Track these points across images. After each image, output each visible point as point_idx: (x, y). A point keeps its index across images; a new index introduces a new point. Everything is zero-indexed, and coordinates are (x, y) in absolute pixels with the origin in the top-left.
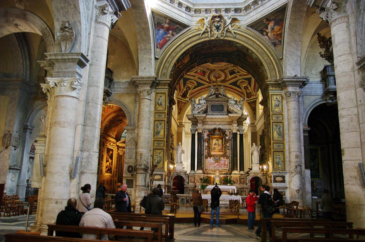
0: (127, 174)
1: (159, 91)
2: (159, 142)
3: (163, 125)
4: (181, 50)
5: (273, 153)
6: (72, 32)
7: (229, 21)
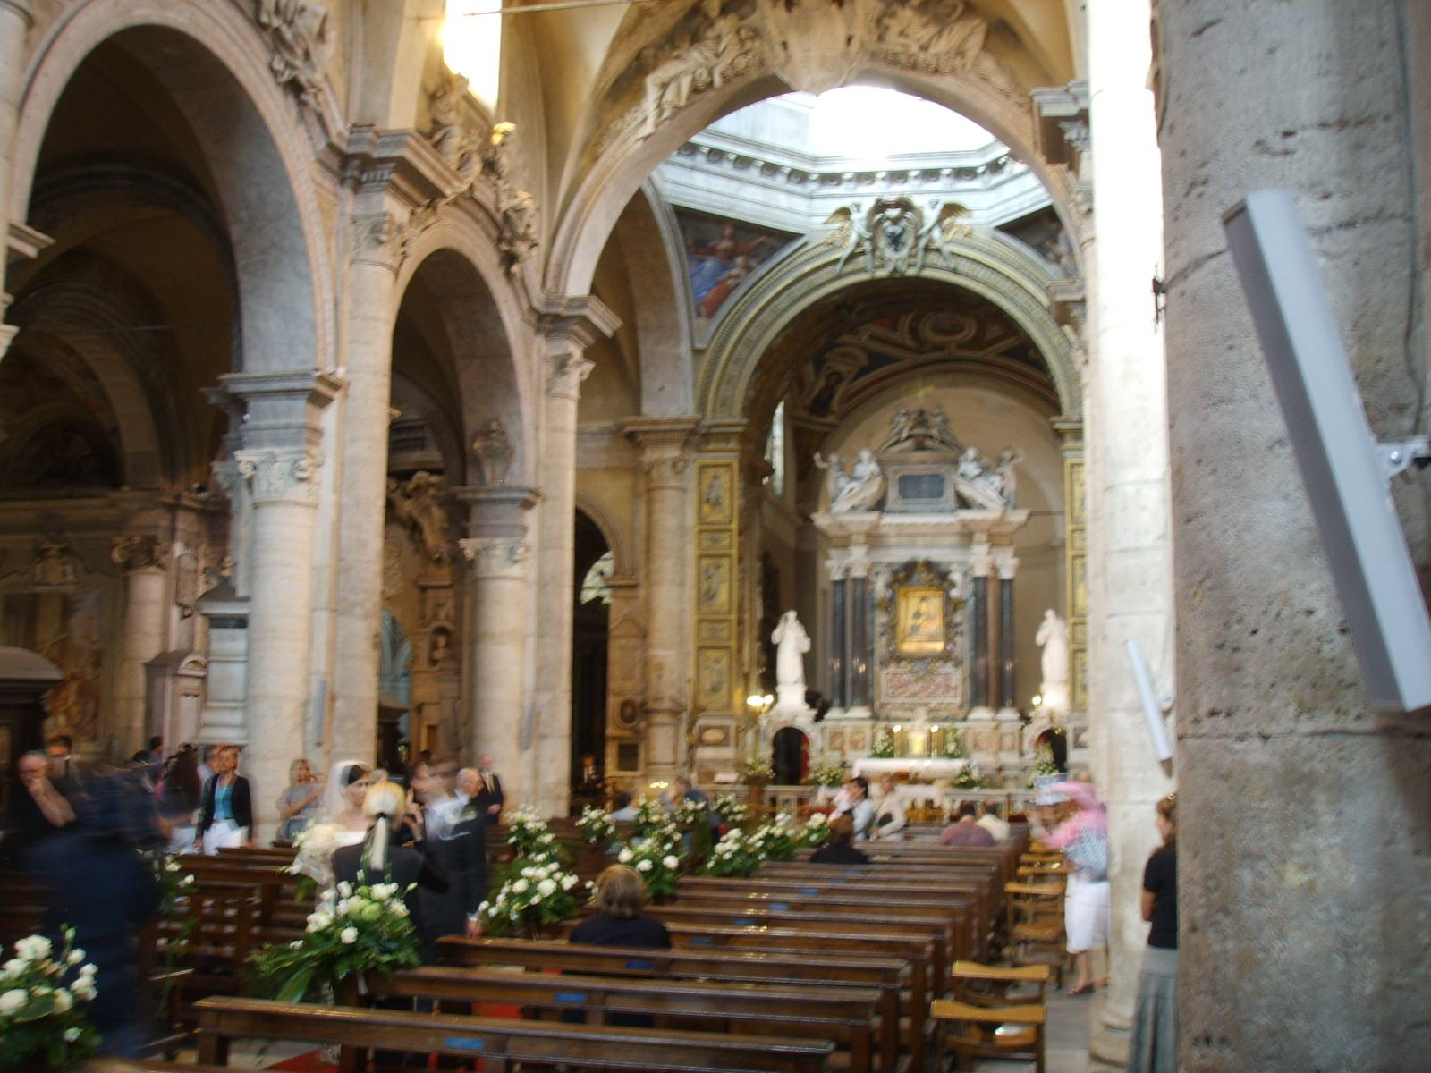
3: (724, 571)
4: (778, 317)
6: (505, 441)
7: (931, 215)
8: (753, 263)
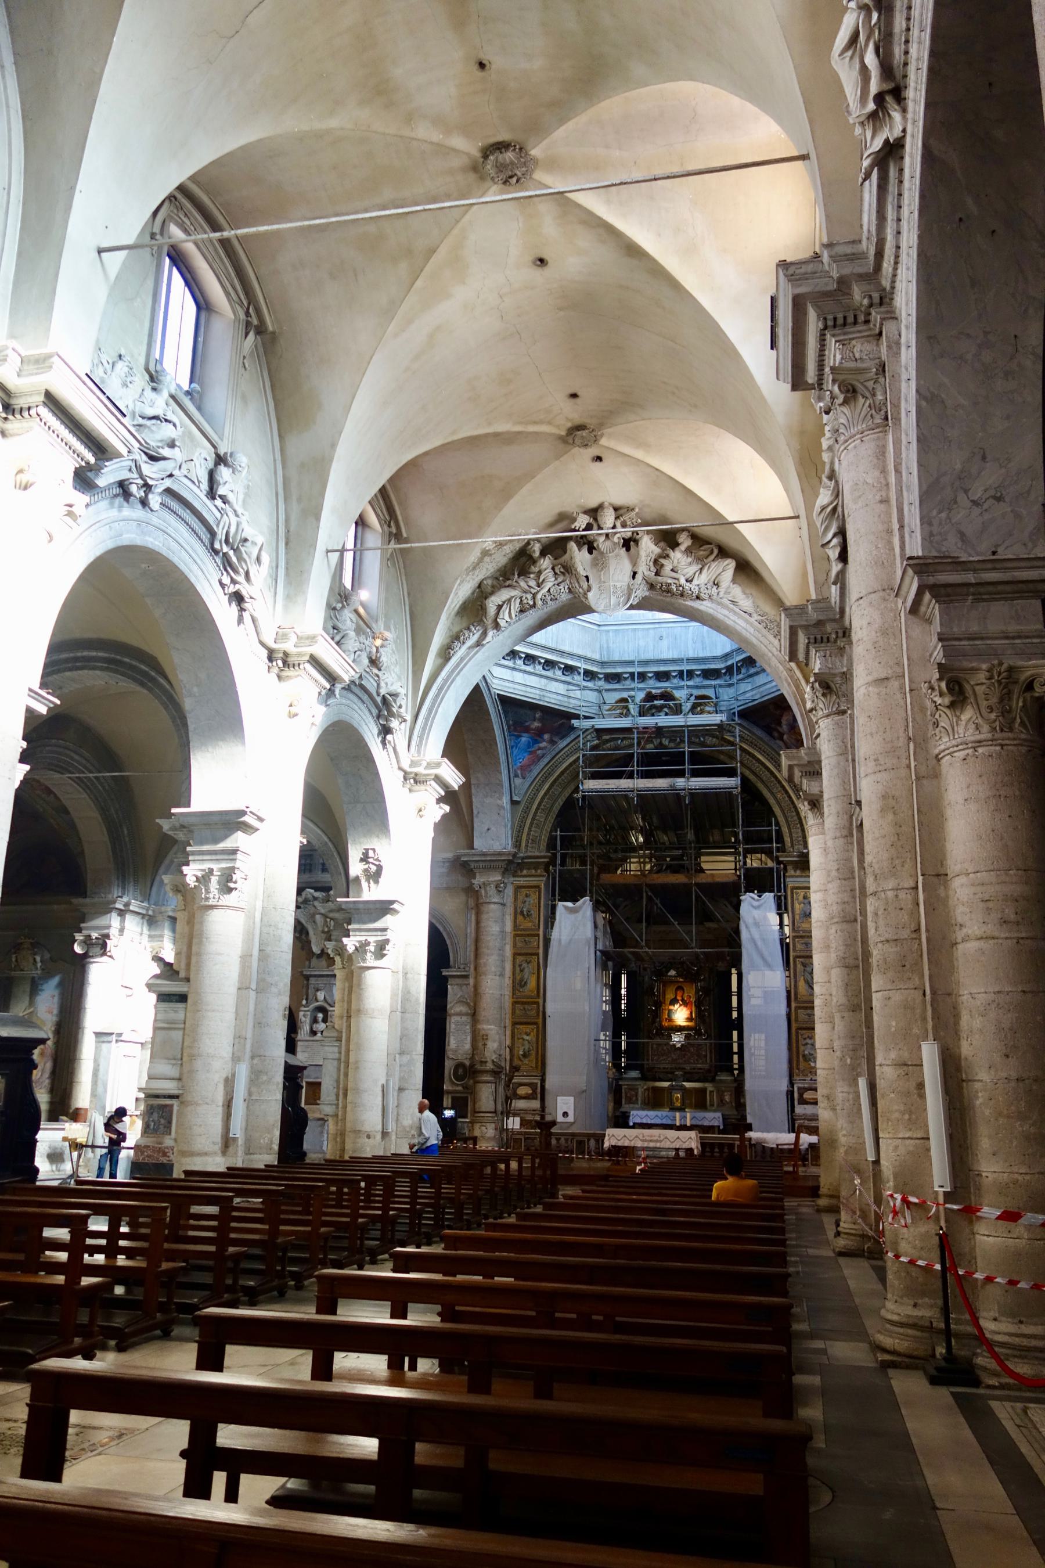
0: (453, 1083)
1: (521, 881)
2: (526, 1007)
5: (797, 1033)
8: (555, 739)
